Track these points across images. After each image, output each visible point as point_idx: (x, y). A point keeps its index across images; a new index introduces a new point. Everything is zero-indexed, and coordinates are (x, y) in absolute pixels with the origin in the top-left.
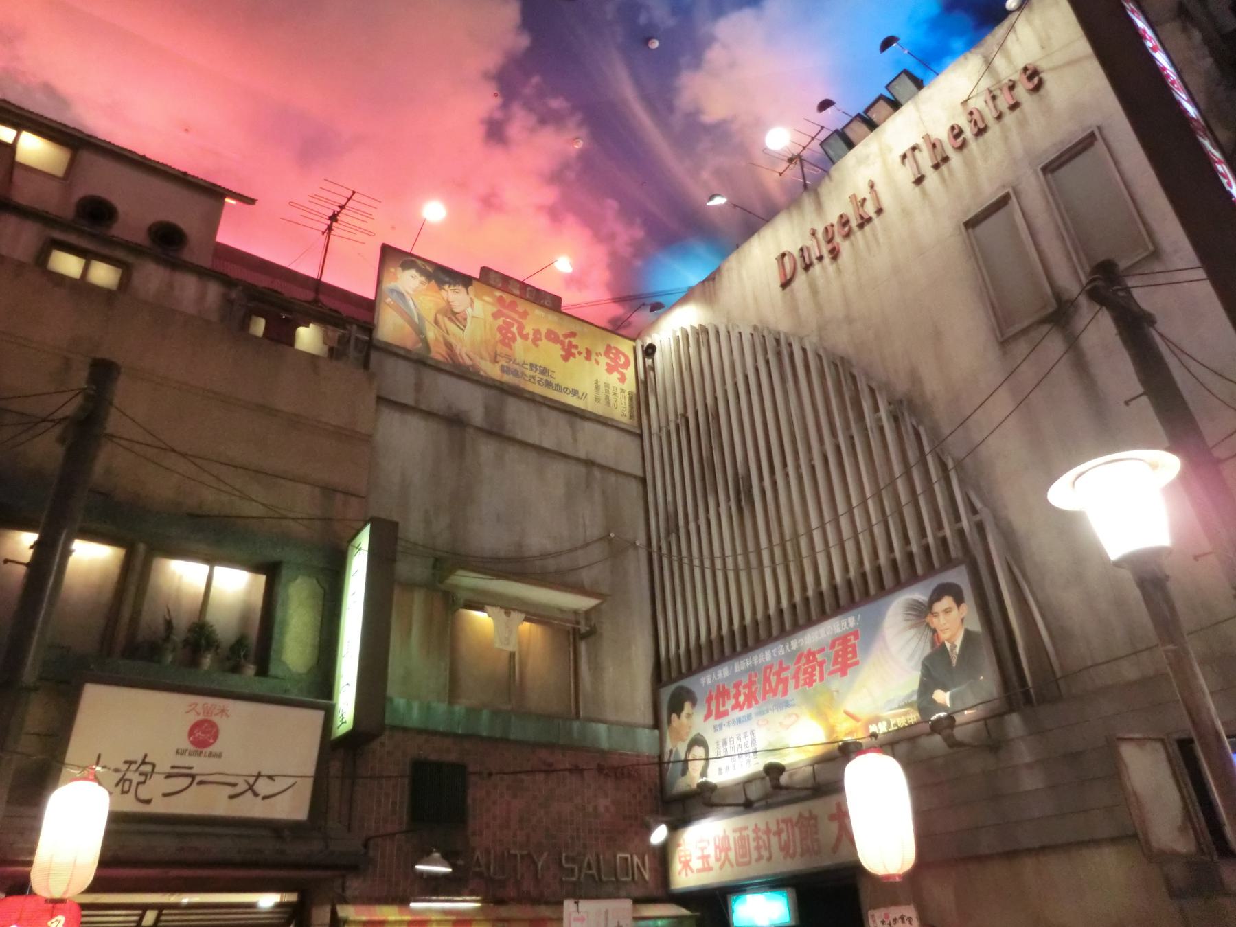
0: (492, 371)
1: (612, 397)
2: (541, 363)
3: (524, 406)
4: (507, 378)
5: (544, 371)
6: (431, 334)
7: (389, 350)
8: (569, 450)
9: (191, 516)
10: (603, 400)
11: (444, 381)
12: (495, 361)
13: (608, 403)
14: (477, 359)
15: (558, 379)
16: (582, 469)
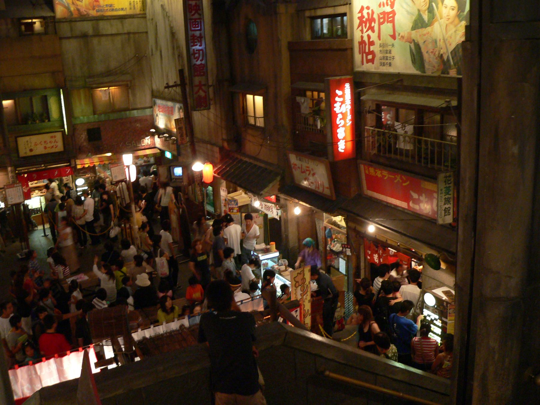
0: (93, 13)
1: (136, 6)
2: (109, 3)
3: (103, 21)
4: (99, 14)
5: (111, 6)
6: (72, 9)
7: (61, 21)
8: (121, 31)
9: (25, 90)
10: (132, 9)
11: (79, 24)
12: (94, 9)
13: (134, 8)
14: (88, 10)
15: (116, 6)
16: (127, 36)
